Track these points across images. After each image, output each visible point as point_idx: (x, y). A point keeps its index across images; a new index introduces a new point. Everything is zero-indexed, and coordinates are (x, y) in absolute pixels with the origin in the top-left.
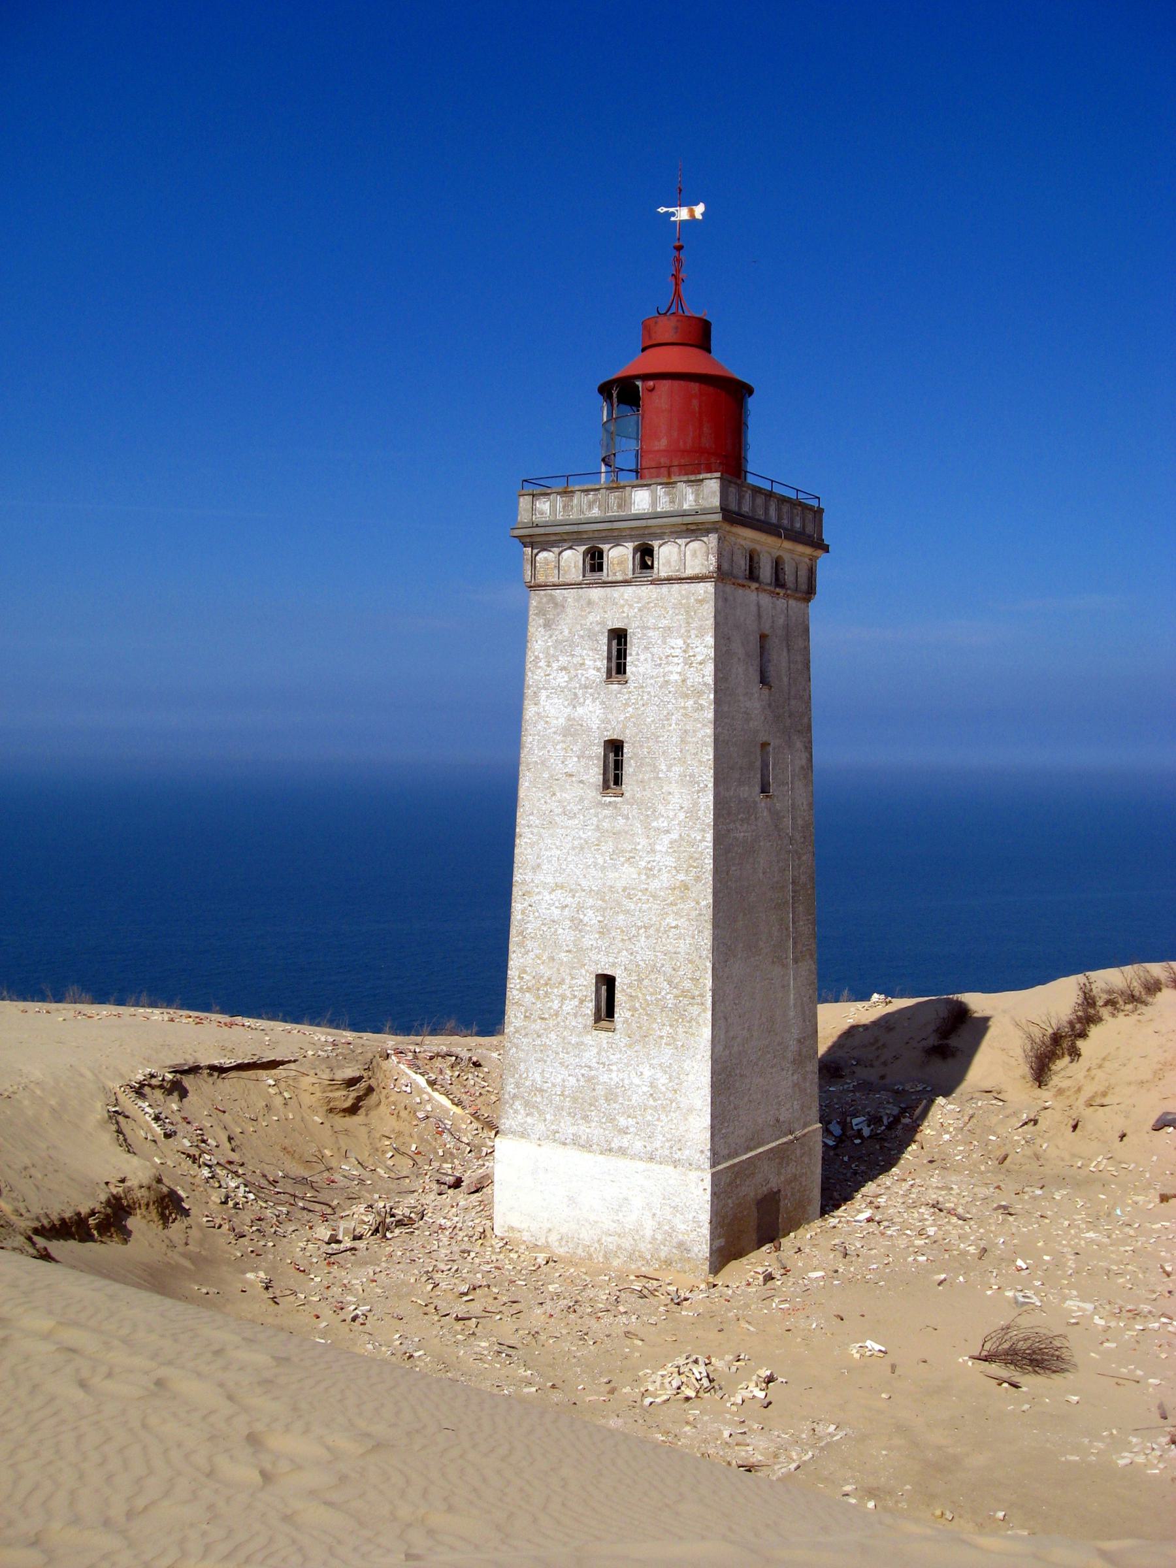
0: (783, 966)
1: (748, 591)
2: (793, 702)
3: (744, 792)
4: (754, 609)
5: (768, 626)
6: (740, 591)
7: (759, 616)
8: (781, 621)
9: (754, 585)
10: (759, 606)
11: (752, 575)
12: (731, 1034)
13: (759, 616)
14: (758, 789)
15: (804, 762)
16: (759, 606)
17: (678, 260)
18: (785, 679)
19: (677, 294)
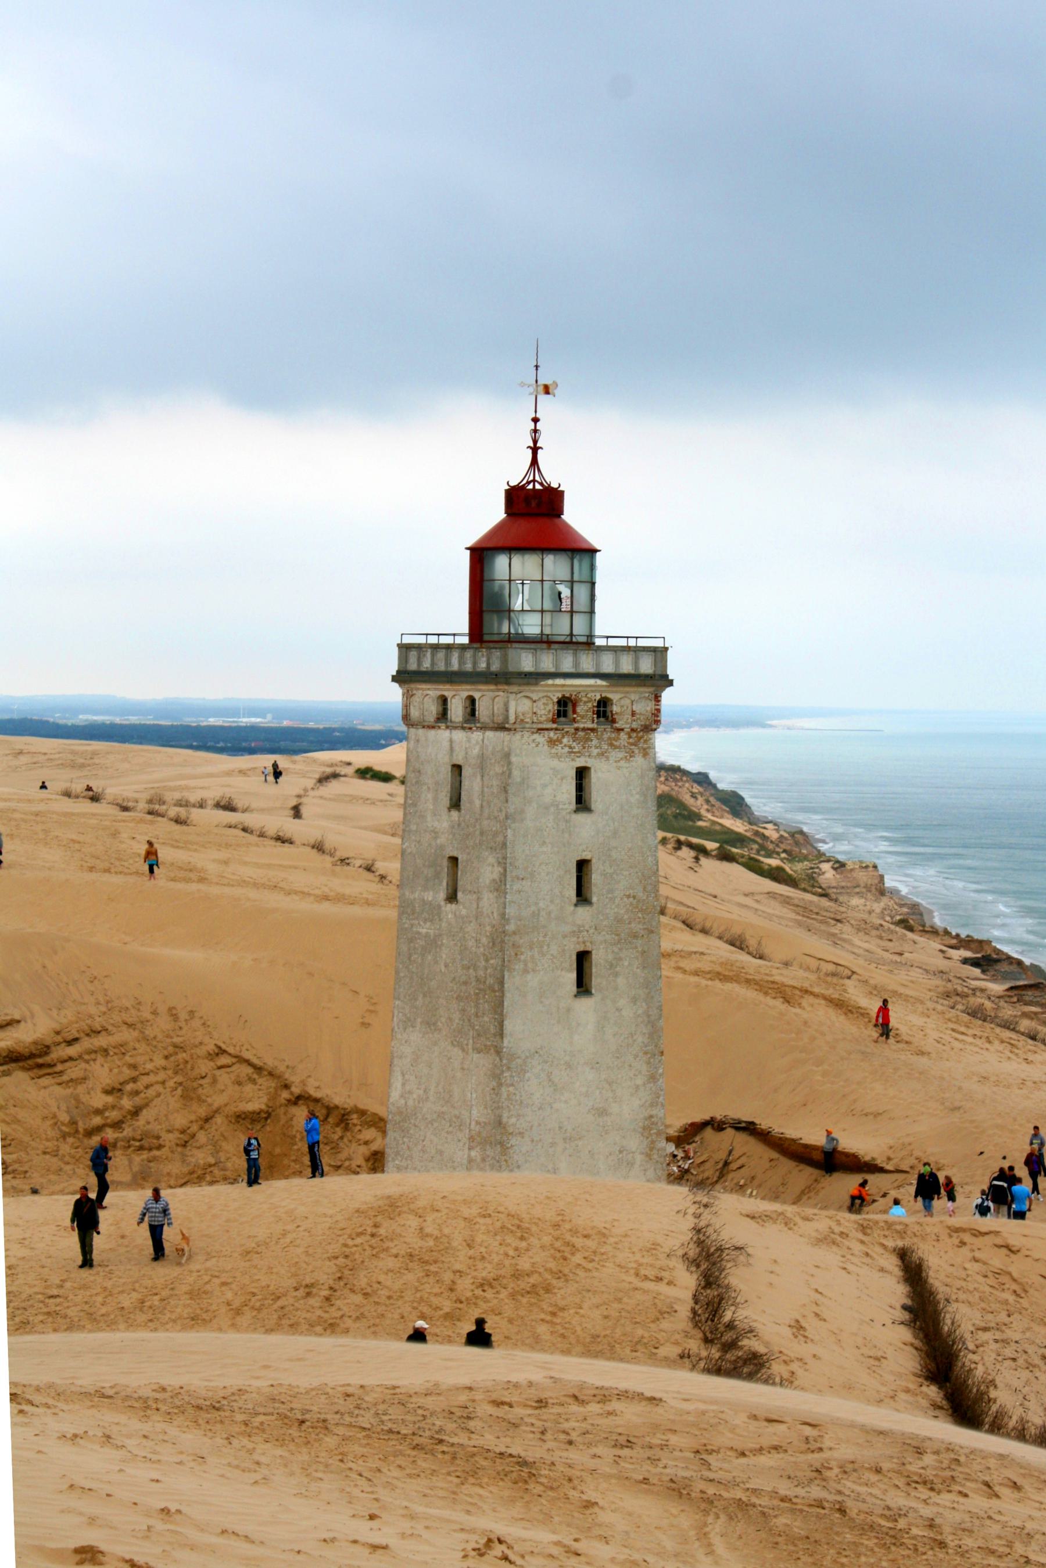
0: (463, 1050)
1: (440, 732)
2: (485, 822)
3: (429, 896)
4: (446, 744)
5: (460, 758)
6: (432, 732)
7: (452, 749)
8: (476, 751)
9: (443, 726)
10: (451, 741)
11: (443, 715)
12: (408, 1088)
13: (452, 749)
14: (442, 895)
15: (496, 876)
16: (451, 741)
17: (535, 431)
18: (477, 803)
19: (534, 462)
